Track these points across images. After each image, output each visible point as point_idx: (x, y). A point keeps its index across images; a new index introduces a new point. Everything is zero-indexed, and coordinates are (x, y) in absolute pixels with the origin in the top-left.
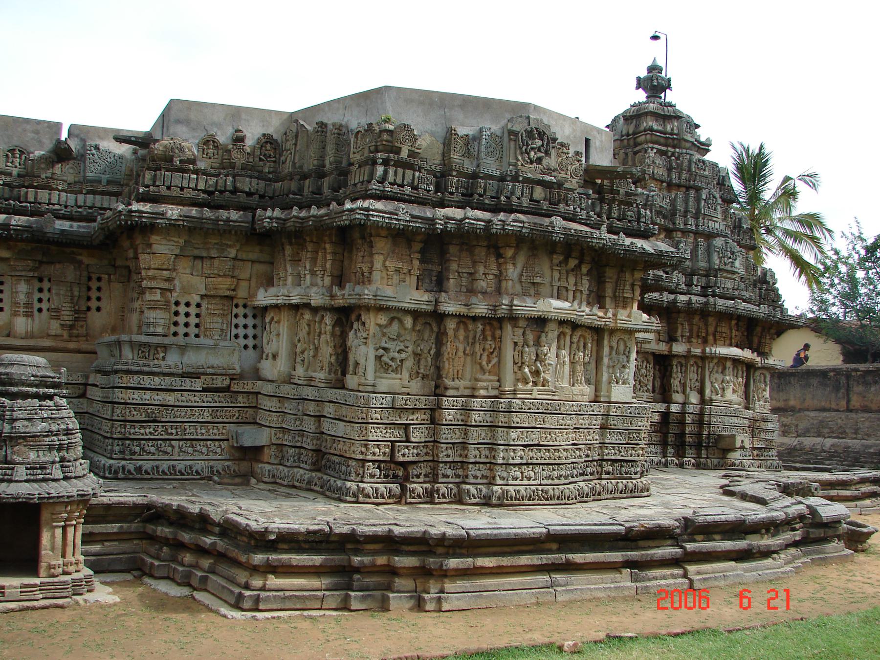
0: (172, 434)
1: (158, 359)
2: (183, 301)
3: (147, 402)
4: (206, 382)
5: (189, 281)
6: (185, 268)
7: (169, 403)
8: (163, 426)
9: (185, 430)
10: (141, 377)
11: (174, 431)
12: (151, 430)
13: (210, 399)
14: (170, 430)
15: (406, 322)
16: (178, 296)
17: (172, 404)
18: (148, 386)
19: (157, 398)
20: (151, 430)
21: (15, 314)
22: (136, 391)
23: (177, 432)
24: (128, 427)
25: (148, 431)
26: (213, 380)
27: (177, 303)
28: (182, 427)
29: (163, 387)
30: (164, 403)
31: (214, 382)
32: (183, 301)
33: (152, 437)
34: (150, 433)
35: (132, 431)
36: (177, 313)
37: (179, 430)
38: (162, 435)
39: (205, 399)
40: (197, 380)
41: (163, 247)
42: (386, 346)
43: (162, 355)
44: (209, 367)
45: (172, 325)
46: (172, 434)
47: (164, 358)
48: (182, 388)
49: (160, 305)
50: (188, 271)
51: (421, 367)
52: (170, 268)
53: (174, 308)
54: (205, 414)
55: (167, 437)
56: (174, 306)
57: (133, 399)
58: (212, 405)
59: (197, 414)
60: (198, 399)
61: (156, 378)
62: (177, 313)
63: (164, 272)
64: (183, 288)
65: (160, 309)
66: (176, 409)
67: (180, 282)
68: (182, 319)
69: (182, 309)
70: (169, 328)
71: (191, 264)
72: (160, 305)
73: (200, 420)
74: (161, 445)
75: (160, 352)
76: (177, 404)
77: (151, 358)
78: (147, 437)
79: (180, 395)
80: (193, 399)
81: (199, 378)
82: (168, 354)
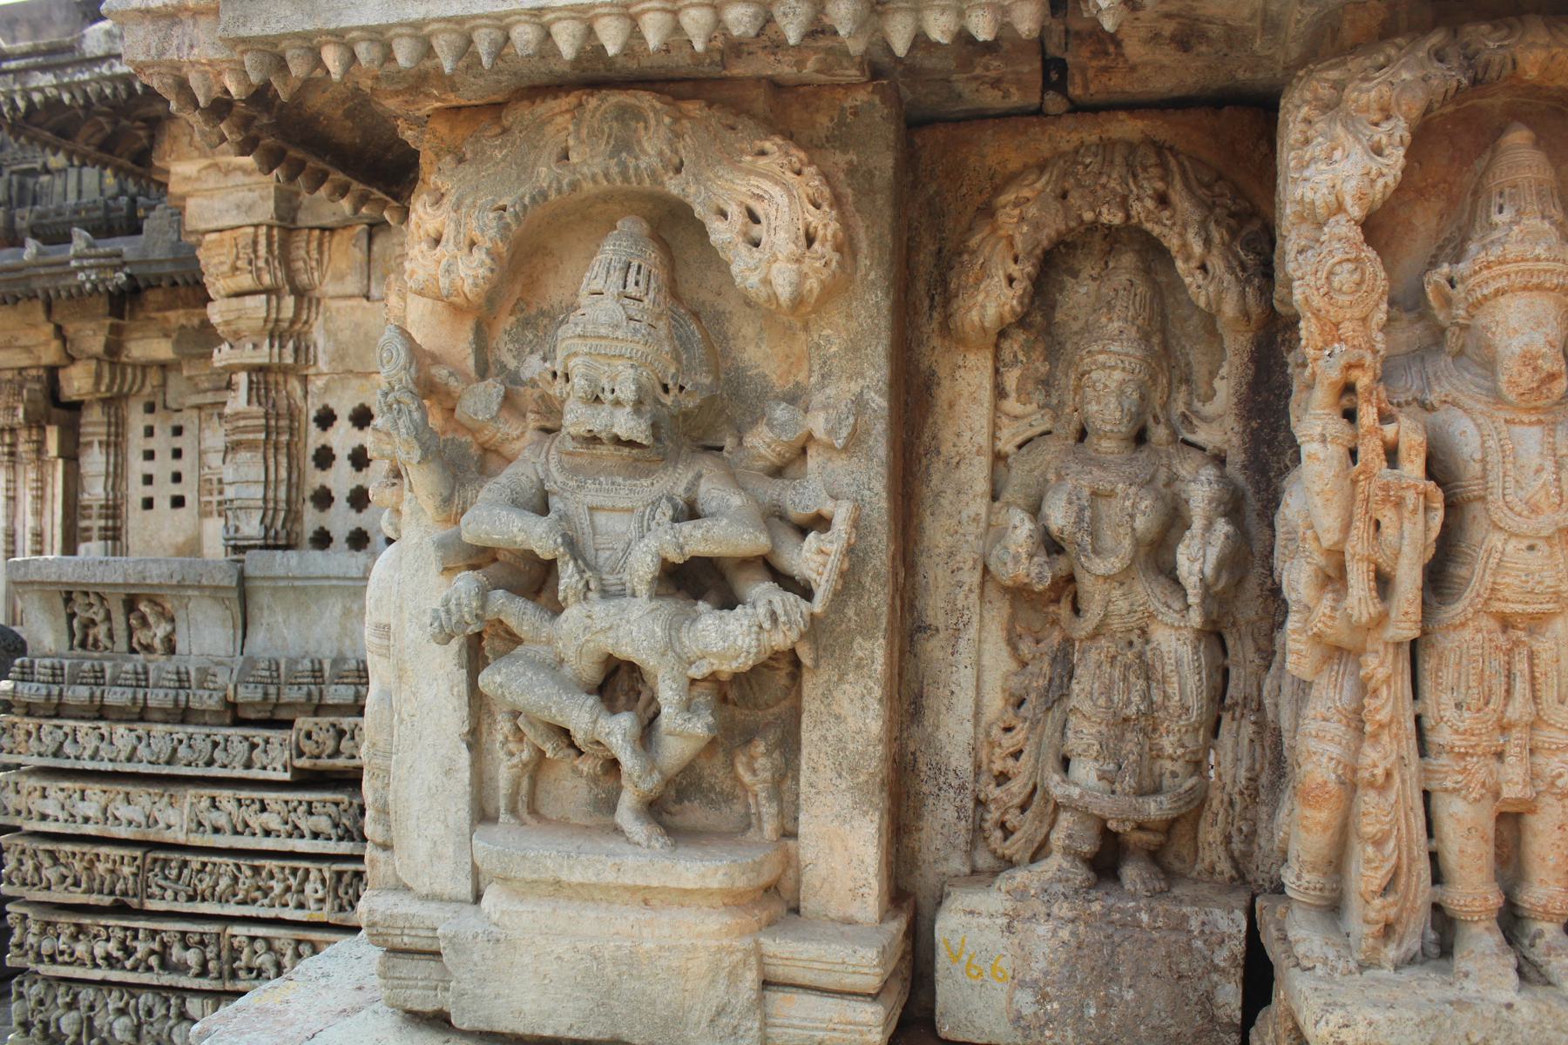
0: (182, 968)
1: (148, 648)
2: (343, 409)
3: (90, 829)
4: (308, 747)
5: (357, 325)
6: (340, 277)
7: (168, 837)
8: (153, 934)
9: (235, 953)
10: (69, 724)
11: (192, 957)
12: (112, 947)
13: (323, 824)
14: (176, 953)
15: (721, 233)
16: (327, 389)
17: (181, 838)
18: (90, 765)
19: (124, 812)
20: (112, 947)
21: (204, 514)
22: (53, 787)
23: (204, 964)
24: (34, 928)
25: (99, 949)
26: (341, 734)
27: (326, 419)
28: (224, 942)
29: (144, 768)
30: (152, 835)
31: (345, 744)
32: (343, 409)
33: (115, 975)
34: (108, 957)
35: (47, 946)
36: (324, 458)
37: (211, 952)
38: (149, 969)
39: (306, 824)
40: (275, 735)
41: (218, 204)
42: (539, 537)
43: (161, 630)
44: (340, 679)
45: (309, 505)
46: (182, 968)
47: (171, 649)
48: (215, 771)
49: (245, 430)
50: (352, 285)
51: (1084, 734)
52: (267, 280)
53: (315, 438)
54: (309, 888)
55: (167, 979)
56: (313, 429)
57: (44, 817)
58: (332, 847)
59: (278, 888)
60: (273, 822)
61: (121, 729)
62: (324, 458)
63: (250, 302)
64: (340, 355)
65: (251, 446)
66: (195, 861)
67: (328, 332)
68: (341, 479)
69: (342, 438)
70: (293, 515)
71: (359, 255)
72: (245, 430)
73: (290, 914)
74: (150, 1013)
75: (151, 619)
76: (197, 840)
77: (122, 645)
78: (97, 975)
79: (205, 803)
80: (256, 821)
81: (288, 724)
82: (181, 627)
